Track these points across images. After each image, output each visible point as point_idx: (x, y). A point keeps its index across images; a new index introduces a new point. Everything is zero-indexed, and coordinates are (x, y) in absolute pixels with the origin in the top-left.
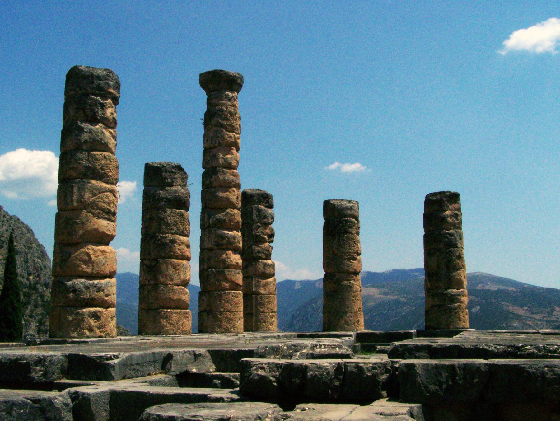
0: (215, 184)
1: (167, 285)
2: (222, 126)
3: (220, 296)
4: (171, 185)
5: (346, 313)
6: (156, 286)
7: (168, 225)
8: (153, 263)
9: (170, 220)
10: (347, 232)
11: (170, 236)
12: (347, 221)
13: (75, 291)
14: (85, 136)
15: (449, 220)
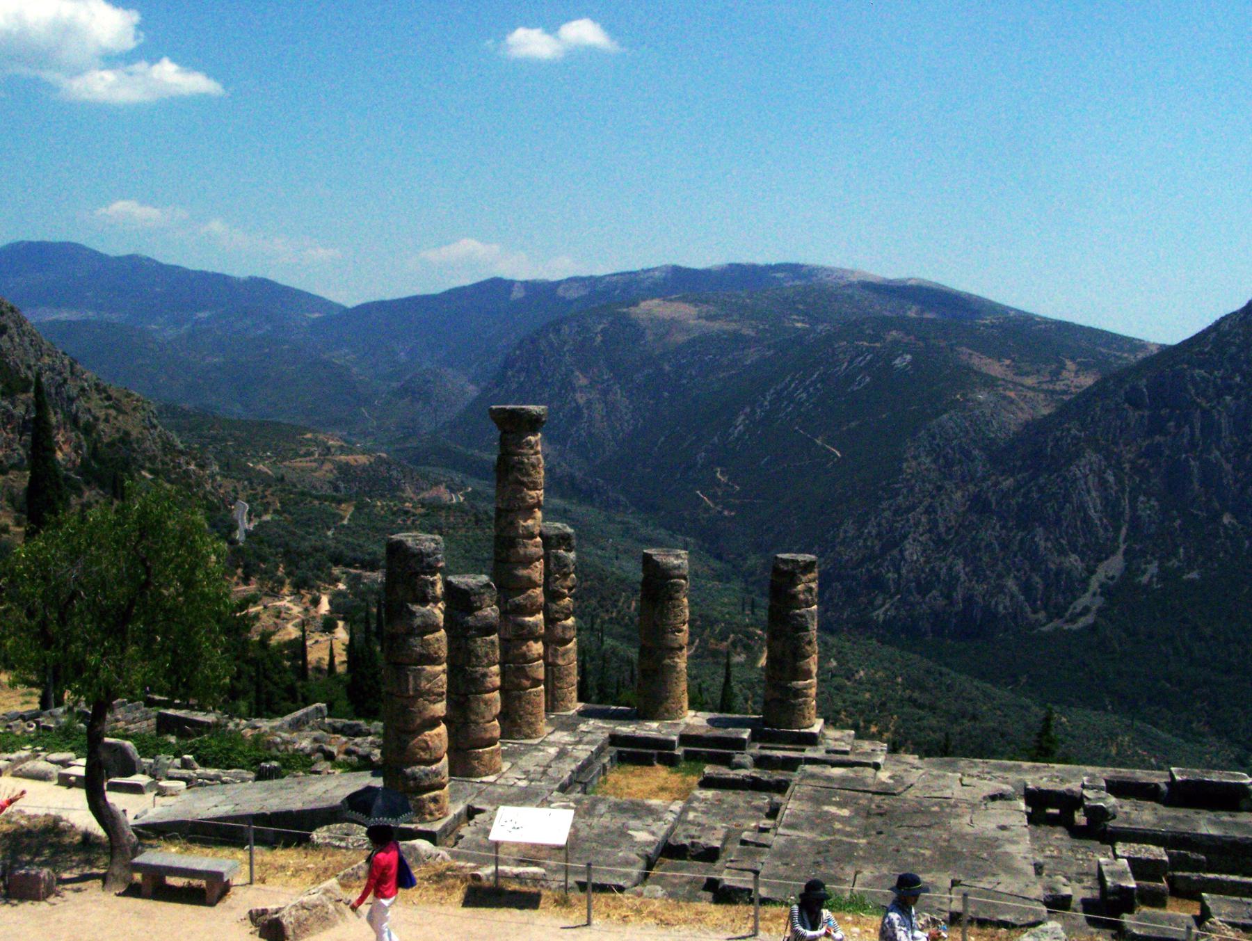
0: (513, 560)
1: (478, 724)
2: (522, 484)
3: (520, 698)
4: (480, 608)
5: (667, 698)
6: (466, 723)
7: (478, 657)
8: (462, 699)
9: (481, 651)
10: (671, 598)
11: (480, 669)
12: (675, 584)
13: (415, 779)
14: (418, 621)
15: (801, 596)
